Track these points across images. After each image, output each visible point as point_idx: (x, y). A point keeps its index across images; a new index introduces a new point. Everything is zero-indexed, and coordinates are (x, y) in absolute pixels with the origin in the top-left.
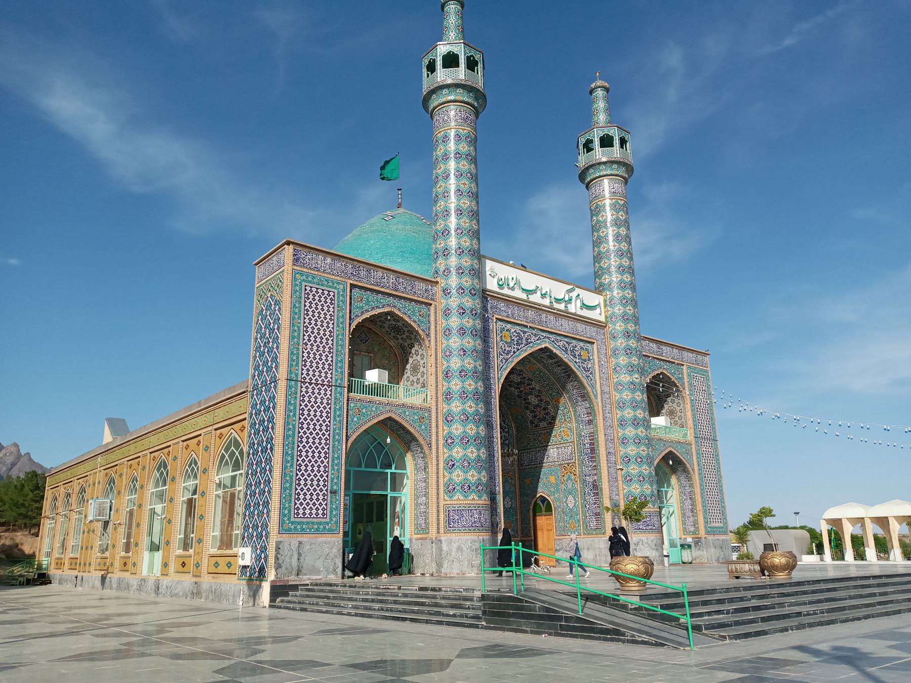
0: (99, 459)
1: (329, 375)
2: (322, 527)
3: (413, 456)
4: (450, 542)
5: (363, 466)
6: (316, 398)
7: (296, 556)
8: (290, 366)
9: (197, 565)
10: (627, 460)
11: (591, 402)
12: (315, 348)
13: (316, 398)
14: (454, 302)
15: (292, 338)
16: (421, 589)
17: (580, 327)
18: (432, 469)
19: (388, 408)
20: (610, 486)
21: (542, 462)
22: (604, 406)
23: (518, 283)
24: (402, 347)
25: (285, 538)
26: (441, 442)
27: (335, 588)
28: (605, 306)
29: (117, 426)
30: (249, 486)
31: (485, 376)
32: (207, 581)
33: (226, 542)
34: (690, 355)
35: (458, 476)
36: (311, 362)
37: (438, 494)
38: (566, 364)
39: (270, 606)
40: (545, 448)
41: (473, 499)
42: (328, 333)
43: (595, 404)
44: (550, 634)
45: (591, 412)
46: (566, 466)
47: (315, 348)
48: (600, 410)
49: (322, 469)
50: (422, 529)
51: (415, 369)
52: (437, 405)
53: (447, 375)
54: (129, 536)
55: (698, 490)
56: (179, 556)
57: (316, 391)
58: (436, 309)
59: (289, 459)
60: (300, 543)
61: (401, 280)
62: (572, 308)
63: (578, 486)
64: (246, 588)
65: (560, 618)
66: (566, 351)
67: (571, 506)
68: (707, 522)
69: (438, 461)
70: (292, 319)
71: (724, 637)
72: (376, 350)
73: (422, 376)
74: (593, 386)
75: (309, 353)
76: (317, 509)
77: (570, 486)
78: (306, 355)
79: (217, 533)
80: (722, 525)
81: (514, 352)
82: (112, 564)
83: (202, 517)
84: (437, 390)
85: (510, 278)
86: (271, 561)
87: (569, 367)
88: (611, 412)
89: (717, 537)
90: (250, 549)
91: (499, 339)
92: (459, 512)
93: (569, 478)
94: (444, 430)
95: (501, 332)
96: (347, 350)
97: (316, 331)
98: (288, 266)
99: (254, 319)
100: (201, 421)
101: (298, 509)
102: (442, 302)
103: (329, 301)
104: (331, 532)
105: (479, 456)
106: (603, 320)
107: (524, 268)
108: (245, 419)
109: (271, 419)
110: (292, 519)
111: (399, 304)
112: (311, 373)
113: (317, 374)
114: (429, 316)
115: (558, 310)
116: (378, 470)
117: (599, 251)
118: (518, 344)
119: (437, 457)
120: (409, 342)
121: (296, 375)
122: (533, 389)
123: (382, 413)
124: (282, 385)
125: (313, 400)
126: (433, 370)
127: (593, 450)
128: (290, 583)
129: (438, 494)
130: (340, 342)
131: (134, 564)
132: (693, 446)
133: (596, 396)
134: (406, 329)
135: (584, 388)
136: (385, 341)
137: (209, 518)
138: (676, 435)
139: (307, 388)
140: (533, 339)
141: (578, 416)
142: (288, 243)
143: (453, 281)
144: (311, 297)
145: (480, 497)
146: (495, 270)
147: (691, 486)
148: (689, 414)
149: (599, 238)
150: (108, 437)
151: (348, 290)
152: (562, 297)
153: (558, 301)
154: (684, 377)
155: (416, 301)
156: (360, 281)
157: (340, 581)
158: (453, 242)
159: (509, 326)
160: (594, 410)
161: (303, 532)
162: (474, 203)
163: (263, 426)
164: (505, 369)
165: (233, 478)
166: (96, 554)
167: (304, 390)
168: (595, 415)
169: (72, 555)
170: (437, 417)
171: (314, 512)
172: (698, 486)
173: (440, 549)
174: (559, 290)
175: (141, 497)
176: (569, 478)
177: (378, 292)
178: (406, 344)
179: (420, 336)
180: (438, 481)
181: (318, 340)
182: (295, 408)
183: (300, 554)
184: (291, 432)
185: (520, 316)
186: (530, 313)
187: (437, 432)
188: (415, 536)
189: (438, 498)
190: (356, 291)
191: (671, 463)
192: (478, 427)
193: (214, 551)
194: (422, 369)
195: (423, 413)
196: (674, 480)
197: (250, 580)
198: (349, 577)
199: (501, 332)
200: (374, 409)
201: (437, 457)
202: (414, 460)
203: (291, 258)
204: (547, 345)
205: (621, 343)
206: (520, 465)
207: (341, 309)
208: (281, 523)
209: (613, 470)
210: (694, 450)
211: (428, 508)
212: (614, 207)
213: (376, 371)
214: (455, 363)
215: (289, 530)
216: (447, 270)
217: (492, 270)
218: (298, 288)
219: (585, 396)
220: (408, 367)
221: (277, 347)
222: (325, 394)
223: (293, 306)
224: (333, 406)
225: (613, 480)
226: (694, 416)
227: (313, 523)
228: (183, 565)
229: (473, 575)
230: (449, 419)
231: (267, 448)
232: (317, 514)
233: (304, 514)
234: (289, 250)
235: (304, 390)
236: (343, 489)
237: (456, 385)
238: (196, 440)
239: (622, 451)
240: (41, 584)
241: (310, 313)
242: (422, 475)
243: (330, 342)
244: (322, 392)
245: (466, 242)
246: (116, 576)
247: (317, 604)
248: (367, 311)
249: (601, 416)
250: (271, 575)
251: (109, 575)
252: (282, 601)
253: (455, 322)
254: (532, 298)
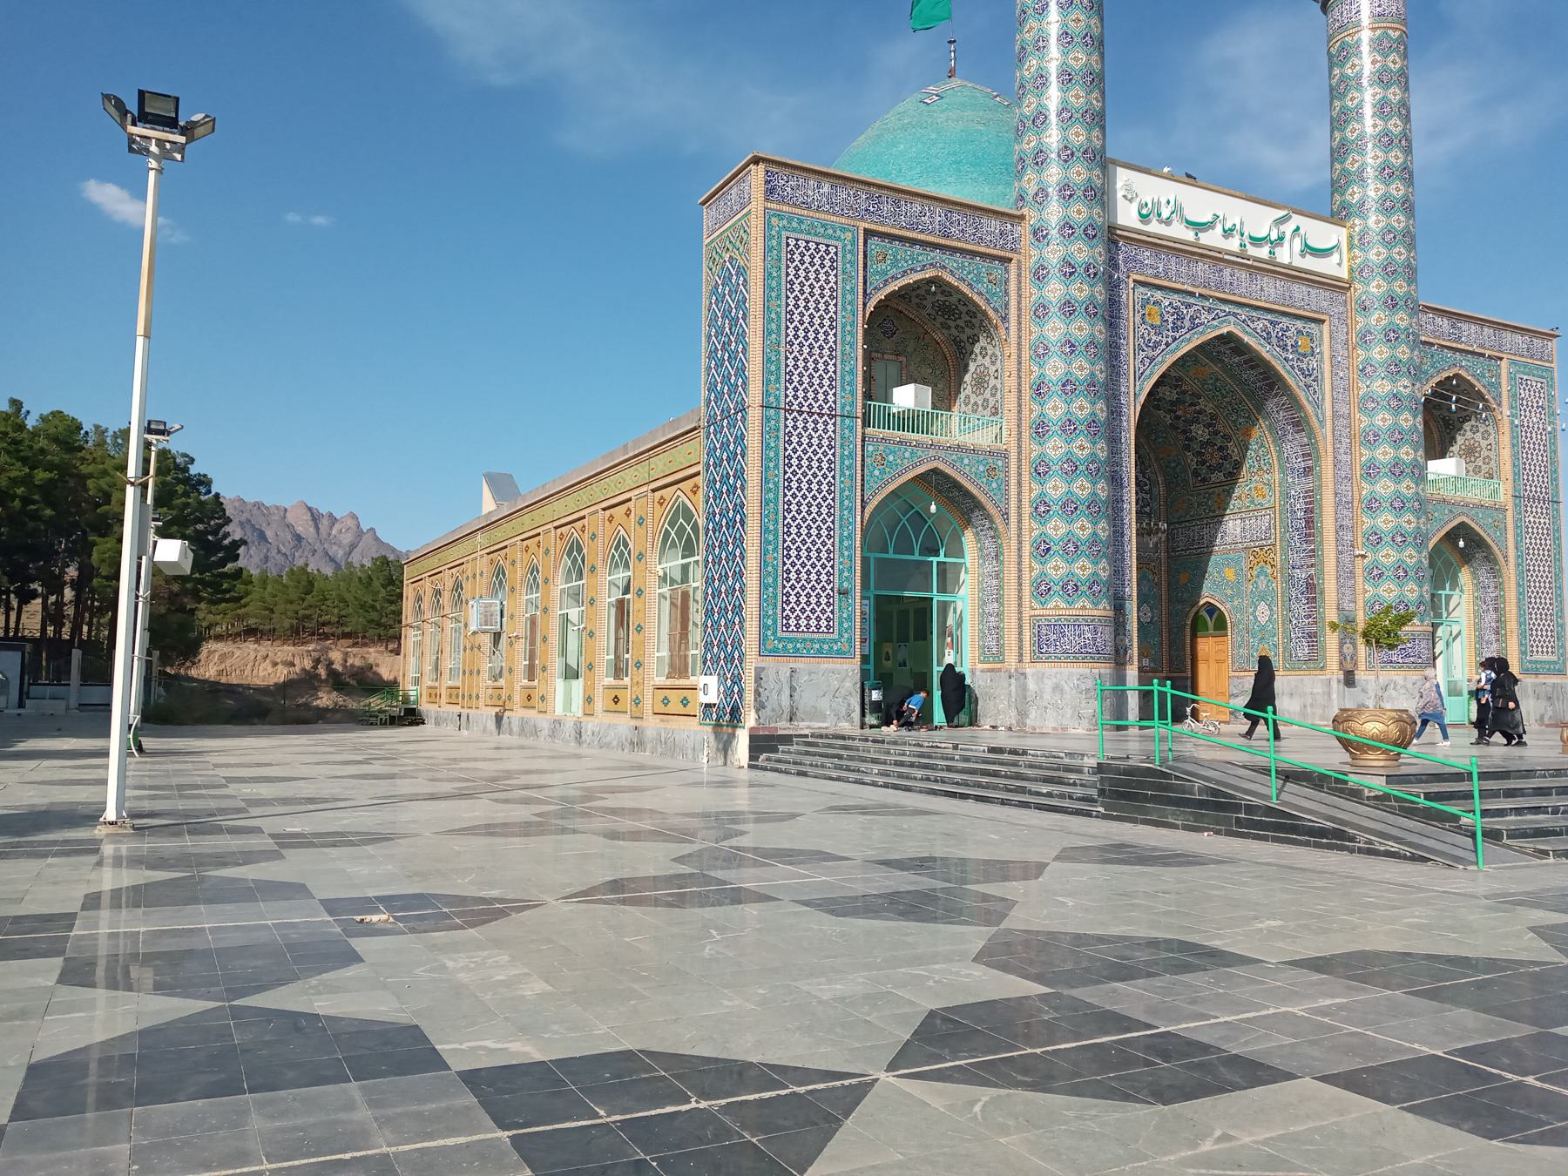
0: (479, 537)
1: (831, 398)
2: (826, 647)
3: (977, 534)
4: (1041, 678)
5: (891, 550)
6: (810, 437)
7: (787, 692)
8: (766, 383)
9: (637, 701)
10: (1375, 539)
11: (1311, 434)
12: (806, 350)
13: (810, 437)
14: (1053, 254)
15: (767, 333)
16: (992, 750)
17: (1299, 291)
18: (1010, 556)
19: (932, 453)
20: (1340, 586)
21: (1211, 544)
22: (1336, 440)
23: (1178, 210)
24: (957, 342)
25: (769, 662)
26: (1027, 510)
27: (850, 743)
28: (1351, 247)
29: (501, 485)
30: (709, 581)
31: (1110, 391)
32: (652, 725)
33: (679, 667)
34: (1518, 338)
35: (1056, 568)
36: (801, 375)
37: (1020, 598)
38: (1267, 364)
39: (750, 766)
40: (1216, 517)
41: (1084, 608)
42: (827, 322)
43: (1320, 438)
44: (1218, 832)
45: (1311, 453)
46: (1258, 551)
47: (806, 350)
48: (1330, 449)
49: (824, 555)
50: (992, 654)
51: (980, 383)
52: (1019, 446)
53: (1039, 391)
54: (532, 656)
55: (1511, 594)
56: (609, 688)
57: (810, 425)
58: (1019, 268)
59: (771, 538)
61: (956, 217)
62: (1283, 256)
63: (1278, 586)
64: (712, 738)
65: (1236, 808)
66: (1268, 339)
67: (1263, 620)
68: (1524, 653)
69: (1020, 543)
70: (767, 300)
71: (1545, 853)
72: (910, 349)
73: (993, 395)
74: (1318, 405)
75: (796, 359)
76: (818, 619)
77: (1262, 586)
78: (791, 362)
79: (665, 653)
80: (1555, 658)
81: (1167, 345)
82: (510, 698)
83: (639, 629)
84: (1020, 419)
85: (1164, 201)
86: (749, 697)
87: (1273, 368)
88: (1349, 451)
89: (1541, 679)
90: (715, 678)
91: (1138, 319)
92: (1058, 628)
93: (1262, 572)
94: (1031, 491)
95: (1143, 307)
96: (860, 352)
97: (806, 319)
98: (757, 204)
99: (705, 302)
100: (629, 476)
101: (788, 618)
102: (1031, 255)
103: (827, 263)
104: (841, 655)
105: (1095, 534)
106: (1345, 276)
107: (1190, 179)
108: (698, 474)
109: (740, 474)
110: (779, 634)
111: (952, 262)
112: (801, 394)
113: (811, 395)
114: (1007, 282)
115: (1256, 260)
116: (916, 557)
117: (1343, 138)
118: (1175, 328)
119: (1019, 536)
120: (968, 331)
121: (777, 398)
122: (1199, 412)
123: (921, 462)
124: (754, 414)
125: (805, 440)
126: (1013, 382)
127: (1309, 522)
128: (780, 732)
129: (1020, 598)
130: (848, 338)
131: (543, 698)
132: (1509, 514)
133: (1322, 423)
134: (963, 309)
135: (1301, 407)
136: (927, 332)
137: (651, 628)
138: (1477, 492)
139: (795, 420)
140: (1205, 317)
141: (1284, 461)
142: (756, 161)
143: (1054, 213)
144: (797, 257)
145: (1096, 604)
146: (1134, 187)
147: (1499, 587)
148: (1506, 454)
149: (1344, 111)
150: (488, 504)
151: (861, 241)
152: (1263, 234)
153: (1256, 242)
154: (1502, 382)
155: (983, 256)
156: (882, 224)
157: (857, 732)
158: (1053, 137)
159: (1158, 295)
160: (1318, 451)
161: (797, 654)
162: (1095, 57)
163: (727, 485)
164: (1149, 377)
165: (685, 568)
166: (485, 681)
168: (1319, 458)
169: (450, 683)
170: (1019, 467)
171: (813, 623)
172: (1513, 585)
173: (1024, 688)
174: (1260, 220)
175: (546, 595)
176: (1262, 572)
177: (913, 242)
178: (964, 337)
179: (990, 321)
180: (1020, 577)
181: (811, 335)
182: (777, 454)
183: (793, 689)
184: (771, 496)
185: (1180, 274)
186: (1201, 268)
187: (1019, 493)
188: (980, 666)
189: (1020, 605)
190: (874, 242)
191: (1461, 544)
192: (1094, 484)
193: (661, 680)
194: (992, 382)
195: (994, 459)
196: (1465, 576)
197: (718, 725)
198: (872, 727)
199: (1143, 307)
200: (907, 455)
201: (1019, 536)
202: (978, 541)
203: (762, 188)
204: (1231, 328)
205: (1379, 320)
206: (1170, 550)
207: (848, 277)
208: (762, 640)
209: (1346, 559)
210: (1510, 520)
211: (1002, 621)
212: (1378, 45)
213: (911, 387)
214: (1055, 368)
215: (776, 650)
216: (1042, 192)
217: (1128, 187)
218: (774, 243)
219: (1300, 424)
220: (967, 378)
221: (744, 351)
222: (825, 431)
223: (768, 276)
224: (838, 451)
225: (1346, 575)
226: (1515, 456)
227: (812, 640)
228: (616, 700)
229: (1080, 731)
230: (1041, 470)
231: (736, 521)
232: (818, 627)
233: (798, 626)
234: (758, 172)
235: (790, 423)
236: (858, 587)
237: (1055, 409)
238: (624, 508)
239: (1367, 522)
240: (411, 724)
241: (797, 287)
242: (990, 567)
243: (831, 338)
244: (820, 426)
245: (1079, 136)
246: (516, 715)
247: (823, 766)
248: (895, 278)
249: (1330, 459)
250: (750, 719)
251: (507, 714)
252: (768, 759)
253: (1055, 290)
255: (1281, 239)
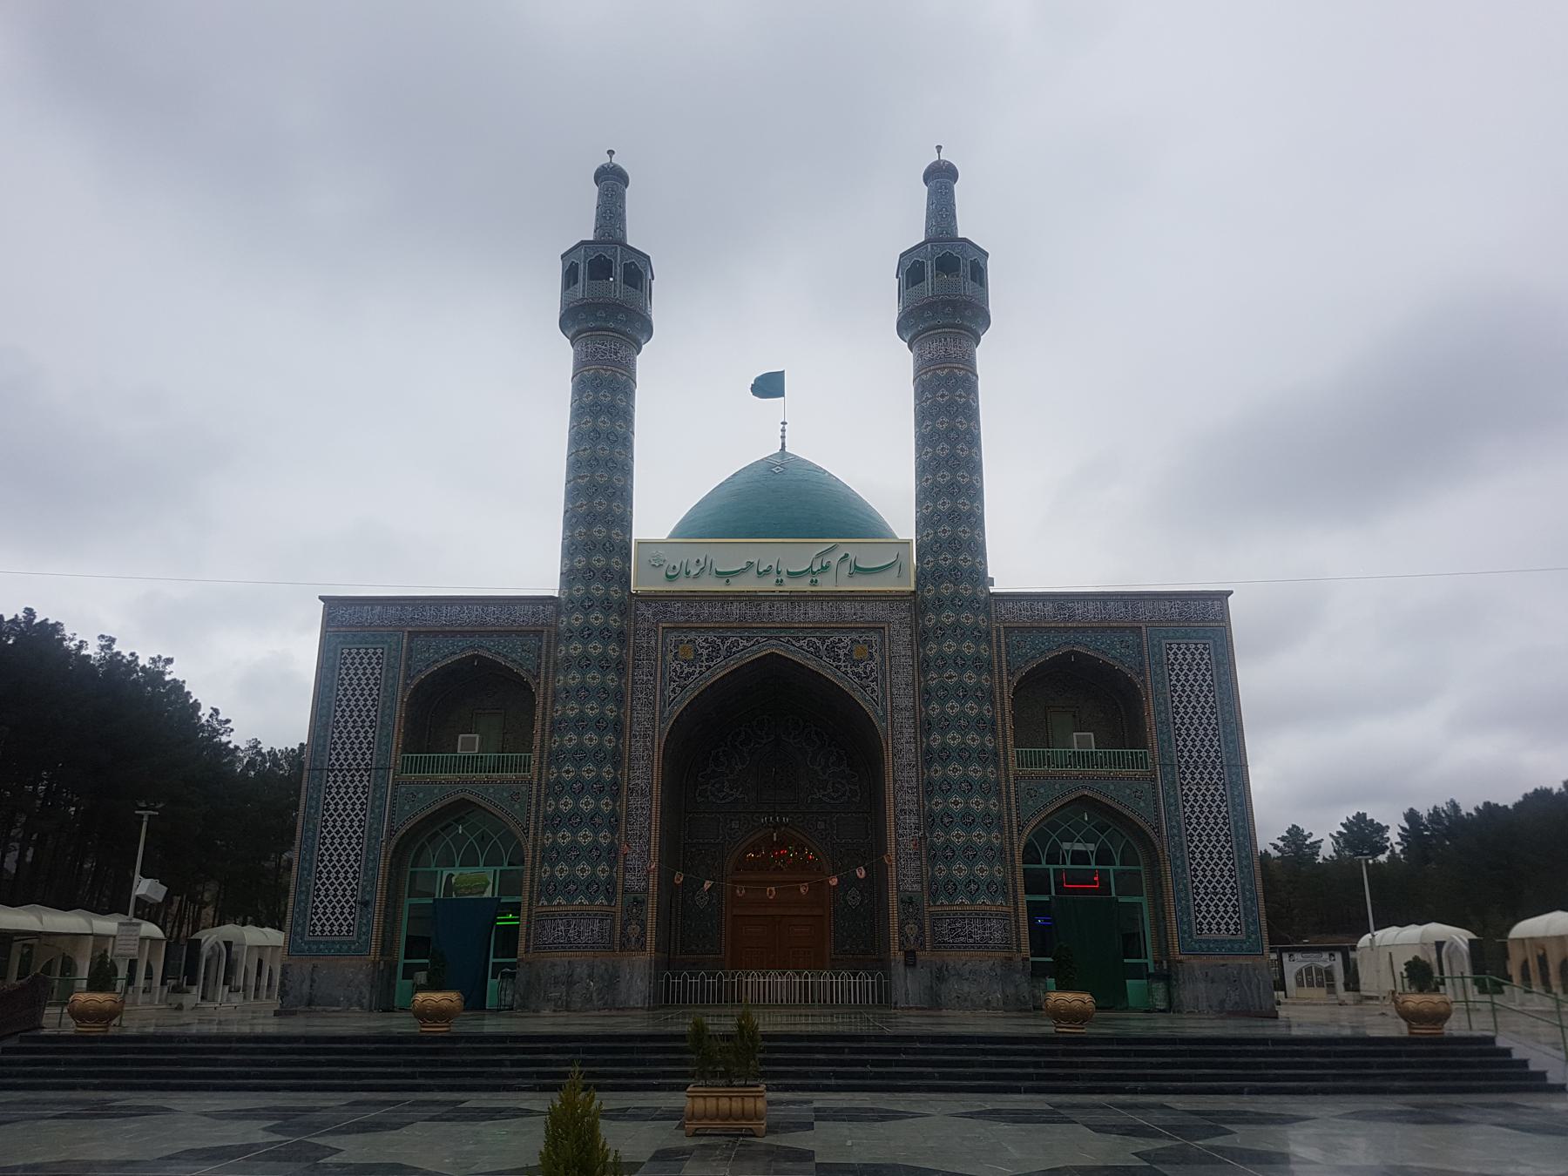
1: (368, 756)
7: (308, 982)
19: (460, 787)
60: (315, 967)
62: (827, 584)
159: (692, 635)
167: (331, 779)
183: (313, 981)
186: (735, 609)
199: (676, 647)
232: (340, 931)
233: (322, 931)
235: (331, 779)
254: (737, 585)
255: (824, 569)
